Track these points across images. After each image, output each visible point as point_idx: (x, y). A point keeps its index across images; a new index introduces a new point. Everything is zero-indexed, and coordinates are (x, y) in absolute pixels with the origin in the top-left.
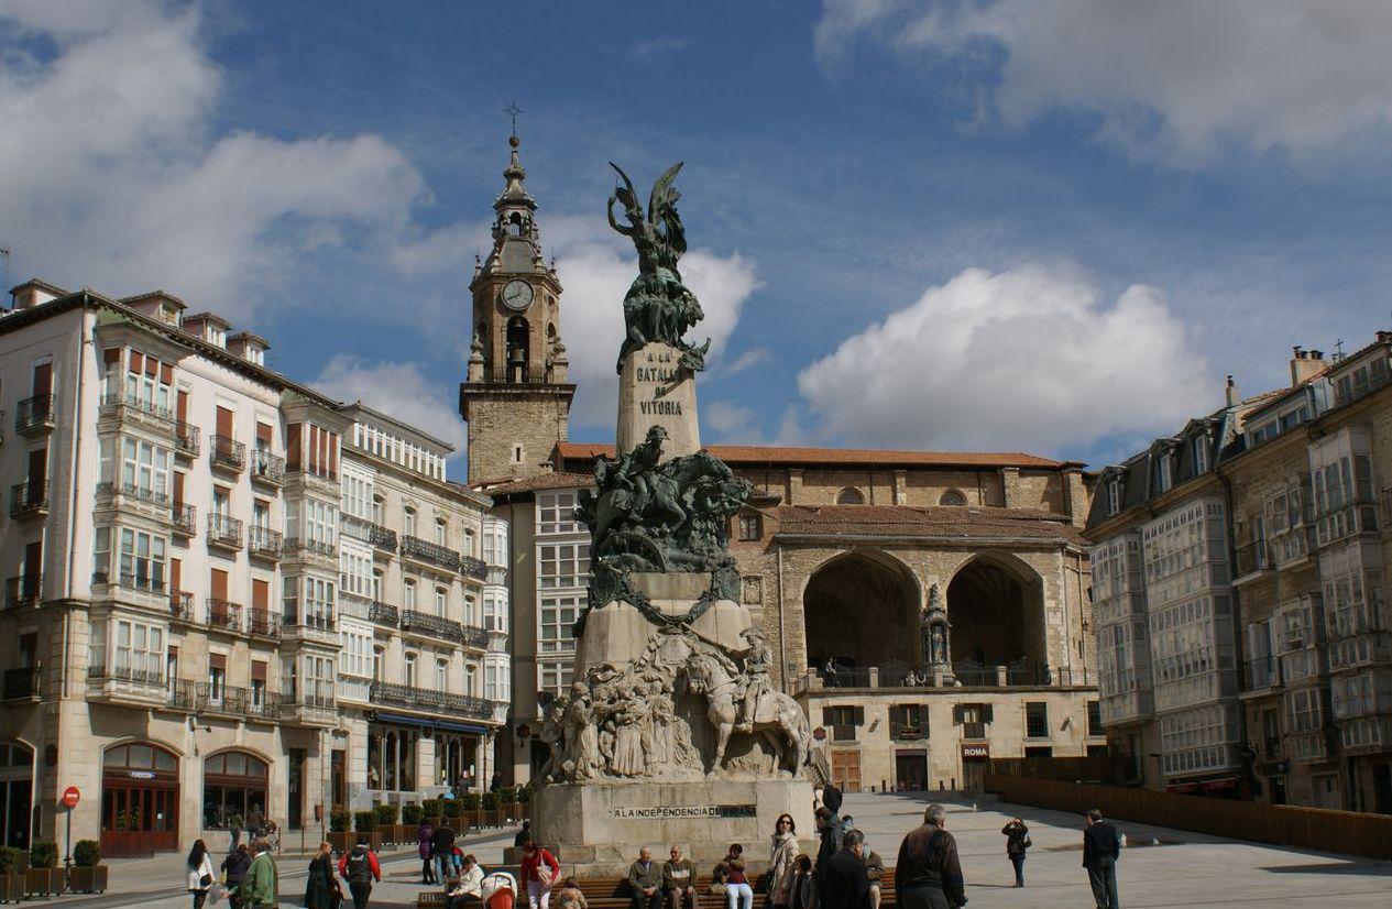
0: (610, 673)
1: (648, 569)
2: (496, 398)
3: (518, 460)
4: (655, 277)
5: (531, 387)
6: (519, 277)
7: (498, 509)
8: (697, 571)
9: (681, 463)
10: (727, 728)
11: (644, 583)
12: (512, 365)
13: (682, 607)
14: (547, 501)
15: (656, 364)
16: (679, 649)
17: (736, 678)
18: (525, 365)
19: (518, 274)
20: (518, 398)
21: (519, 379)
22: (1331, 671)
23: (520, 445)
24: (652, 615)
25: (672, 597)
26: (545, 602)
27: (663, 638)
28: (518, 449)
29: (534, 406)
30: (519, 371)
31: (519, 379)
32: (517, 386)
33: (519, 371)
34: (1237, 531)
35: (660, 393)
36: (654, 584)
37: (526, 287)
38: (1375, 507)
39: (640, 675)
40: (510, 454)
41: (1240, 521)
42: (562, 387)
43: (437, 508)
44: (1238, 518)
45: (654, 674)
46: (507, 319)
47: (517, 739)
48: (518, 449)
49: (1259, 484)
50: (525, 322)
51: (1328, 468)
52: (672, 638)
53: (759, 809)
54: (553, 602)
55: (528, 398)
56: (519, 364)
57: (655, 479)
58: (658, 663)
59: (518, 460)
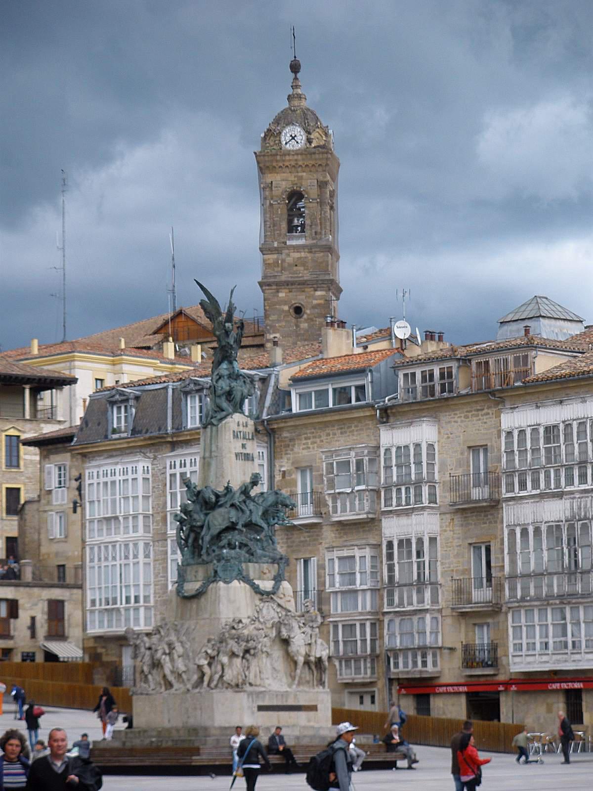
0: (241, 625)
1: (250, 561)
4: (233, 368)
8: (271, 563)
9: (265, 495)
10: (301, 660)
11: (248, 570)
13: (267, 585)
15: (241, 428)
16: (270, 613)
17: (303, 630)
22: (385, 610)
24: (256, 590)
25: (259, 579)
27: (262, 604)
34: (278, 478)
35: (243, 446)
36: (252, 569)
38: (437, 486)
39: (253, 626)
41: (283, 469)
44: (281, 466)
45: (260, 626)
49: (309, 441)
51: (399, 448)
52: (267, 604)
53: (319, 707)
57: (251, 506)
58: (262, 620)
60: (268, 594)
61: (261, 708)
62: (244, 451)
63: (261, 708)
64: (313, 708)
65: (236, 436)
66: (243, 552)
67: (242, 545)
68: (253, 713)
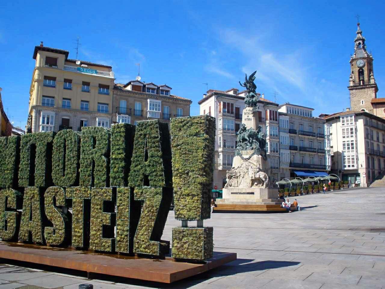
1: (243, 150)
2: (356, 89)
3: (363, 104)
5: (365, 85)
6: (360, 58)
7: (328, 122)
11: (242, 152)
12: (360, 81)
13: (247, 157)
14: (343, 118)
15: (248, 111)
18: (363, 80)
19: (360, 58)
20: (361, 88)
21: (362, 84)
23: (363, 100)
24: (243, 158)
26: (343, 142)
28: (362, 101)
29: (366, 90)
30: (361, 82)
31: (362, 84)
32: (362, 86)
33: (361, 82)
35: (248, 116)
36: (244, 152)
37: (362, 61)
40: (361, 103)
42: (372, 85)
43: (309, 123)
46: (359, 68)
47: (339, 173)
48: (362, 101)
50: (363, 70)
54: (344, 142)
55: (364, 88)
56: (361, 80)
59: (363, 104)
60: (246, 159)
61: (232, 193)
62: (248, 118)
63: (232, 193)
64: (253, 193)
65: (245, 114)
66: (241, 147)
67: (241, 145)
68: (229, 195)
